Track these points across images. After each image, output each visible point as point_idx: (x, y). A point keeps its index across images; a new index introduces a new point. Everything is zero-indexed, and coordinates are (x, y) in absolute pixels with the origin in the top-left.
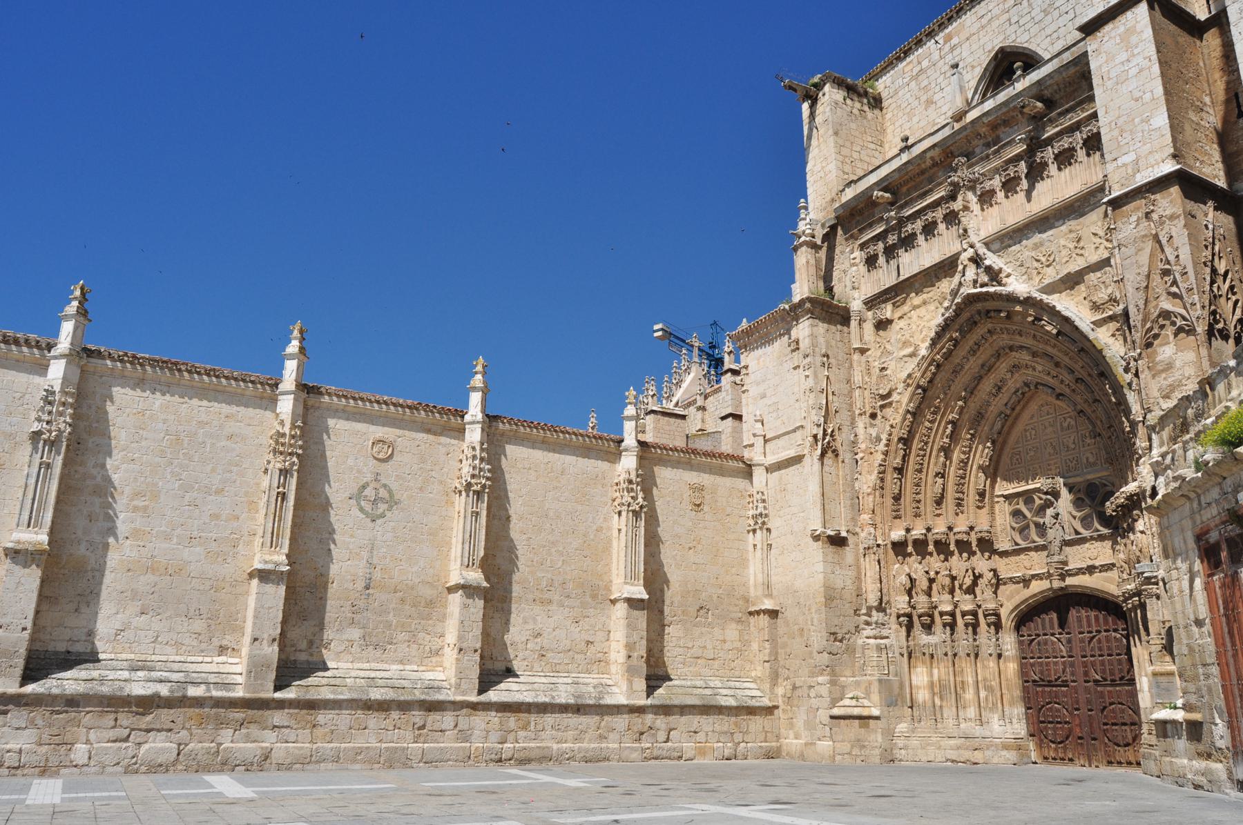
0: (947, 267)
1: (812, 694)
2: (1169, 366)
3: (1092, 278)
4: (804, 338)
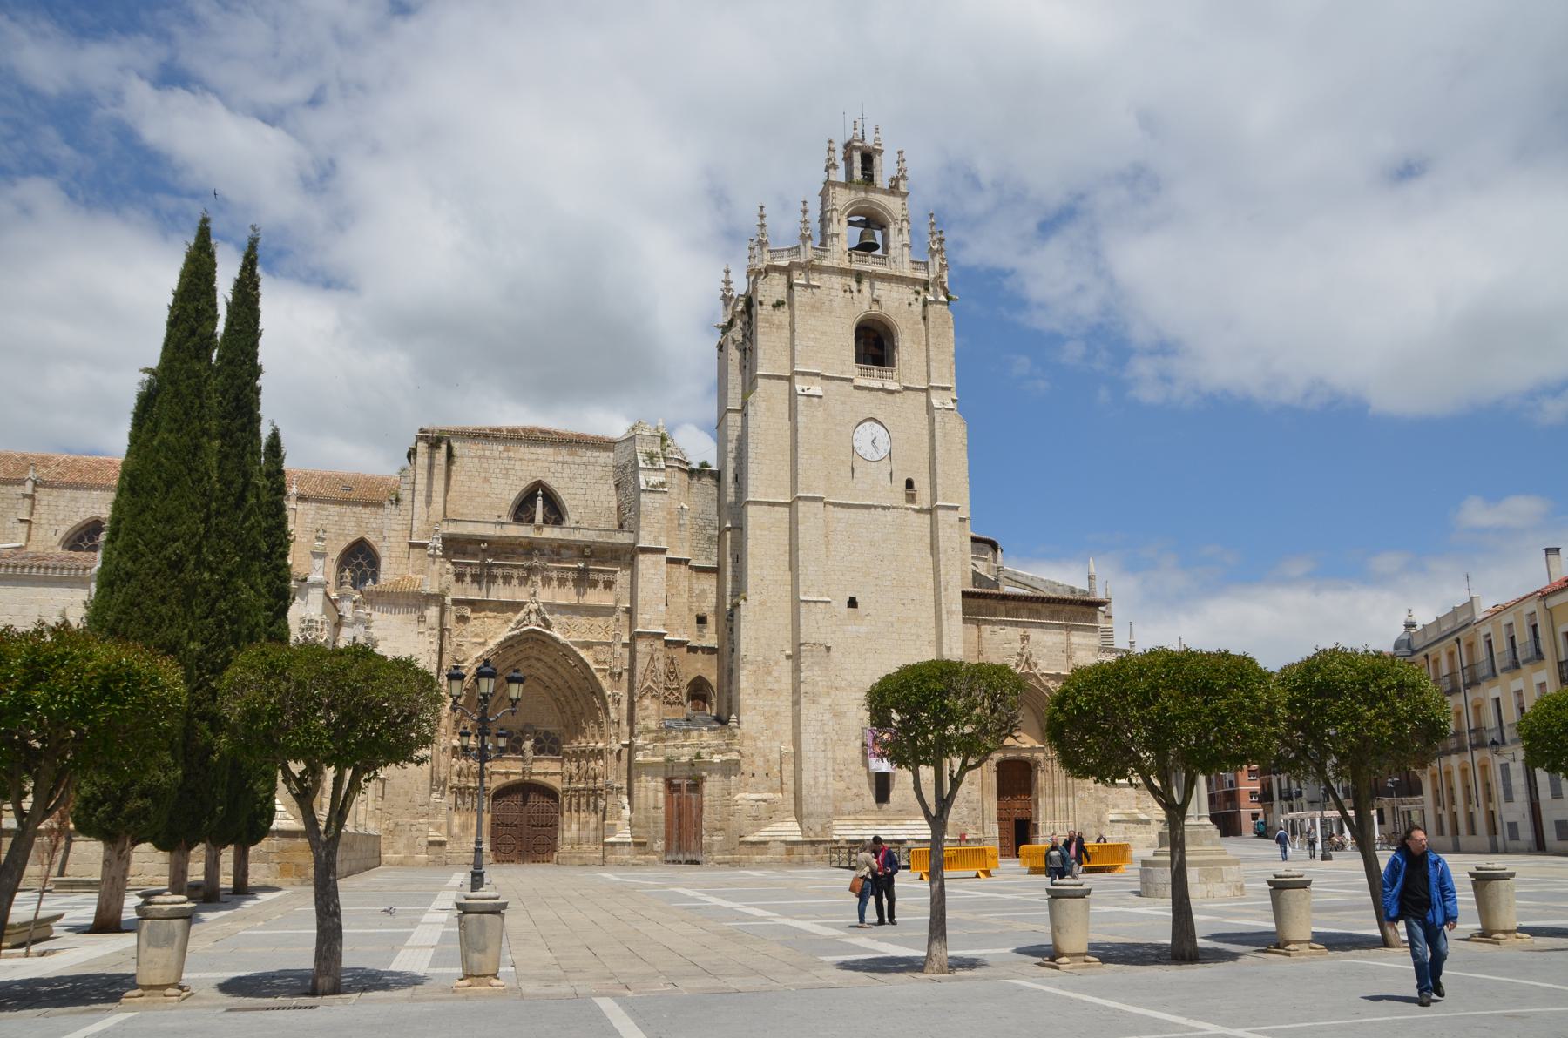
0: (516, 606)
1: (414, 828)
2: (647, 708)
3: (598, 648)
4: (431, 617)
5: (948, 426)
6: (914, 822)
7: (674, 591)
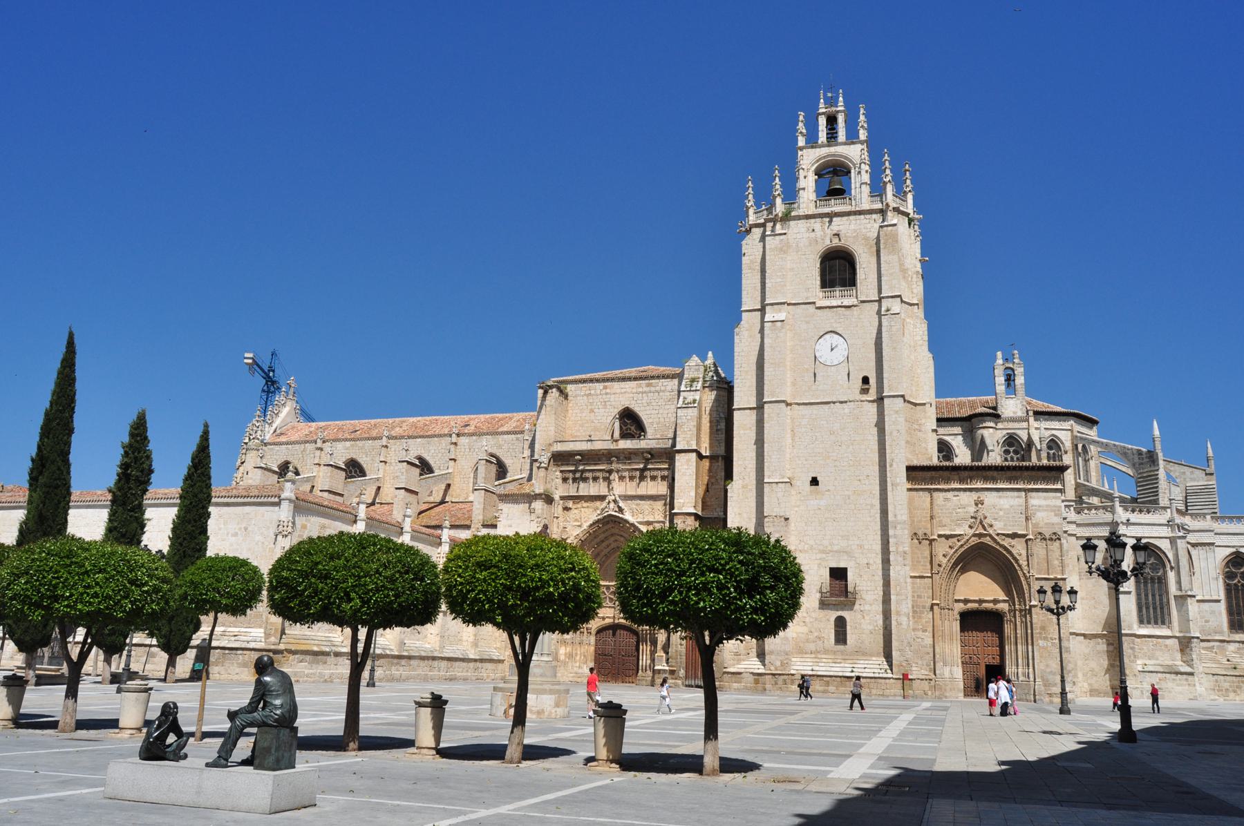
0: (602, 498)
5: (894, 329)
6: (866, 662)
7: (713, 480)
